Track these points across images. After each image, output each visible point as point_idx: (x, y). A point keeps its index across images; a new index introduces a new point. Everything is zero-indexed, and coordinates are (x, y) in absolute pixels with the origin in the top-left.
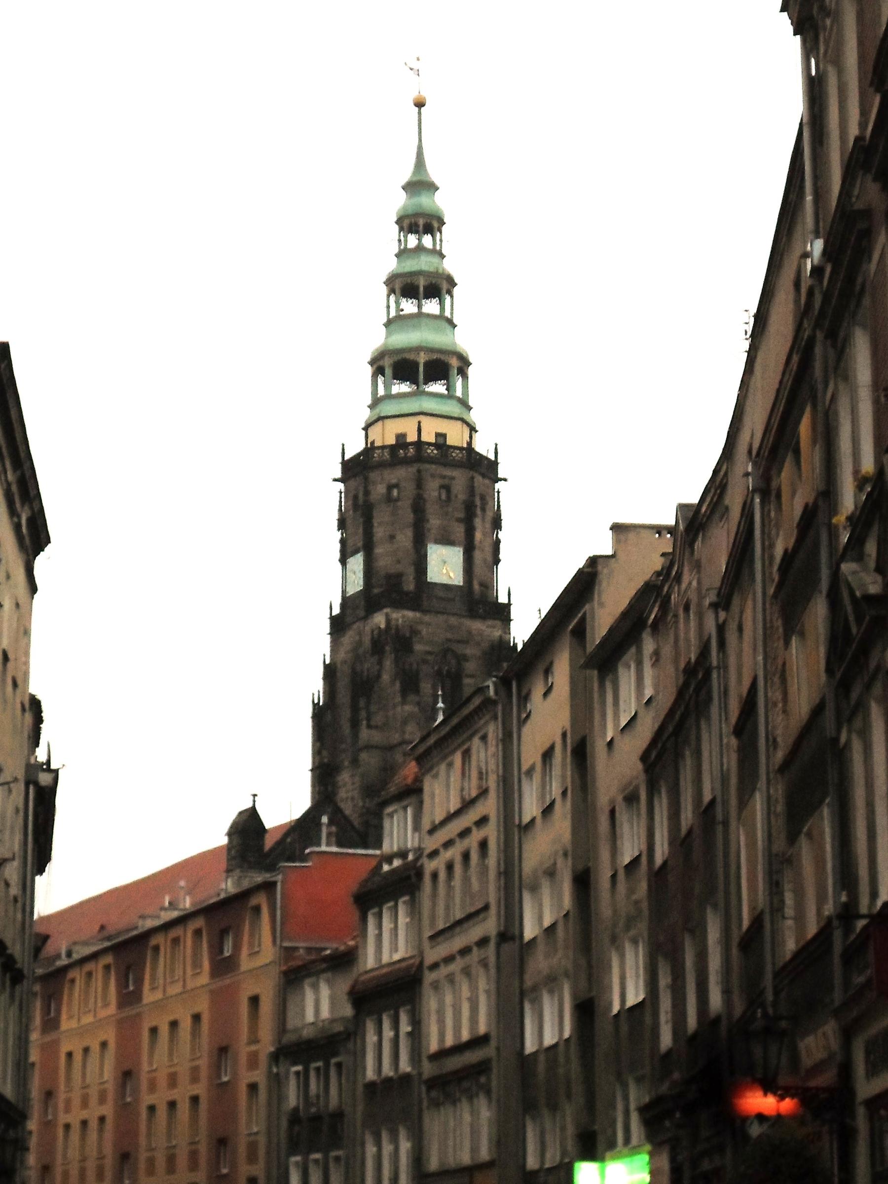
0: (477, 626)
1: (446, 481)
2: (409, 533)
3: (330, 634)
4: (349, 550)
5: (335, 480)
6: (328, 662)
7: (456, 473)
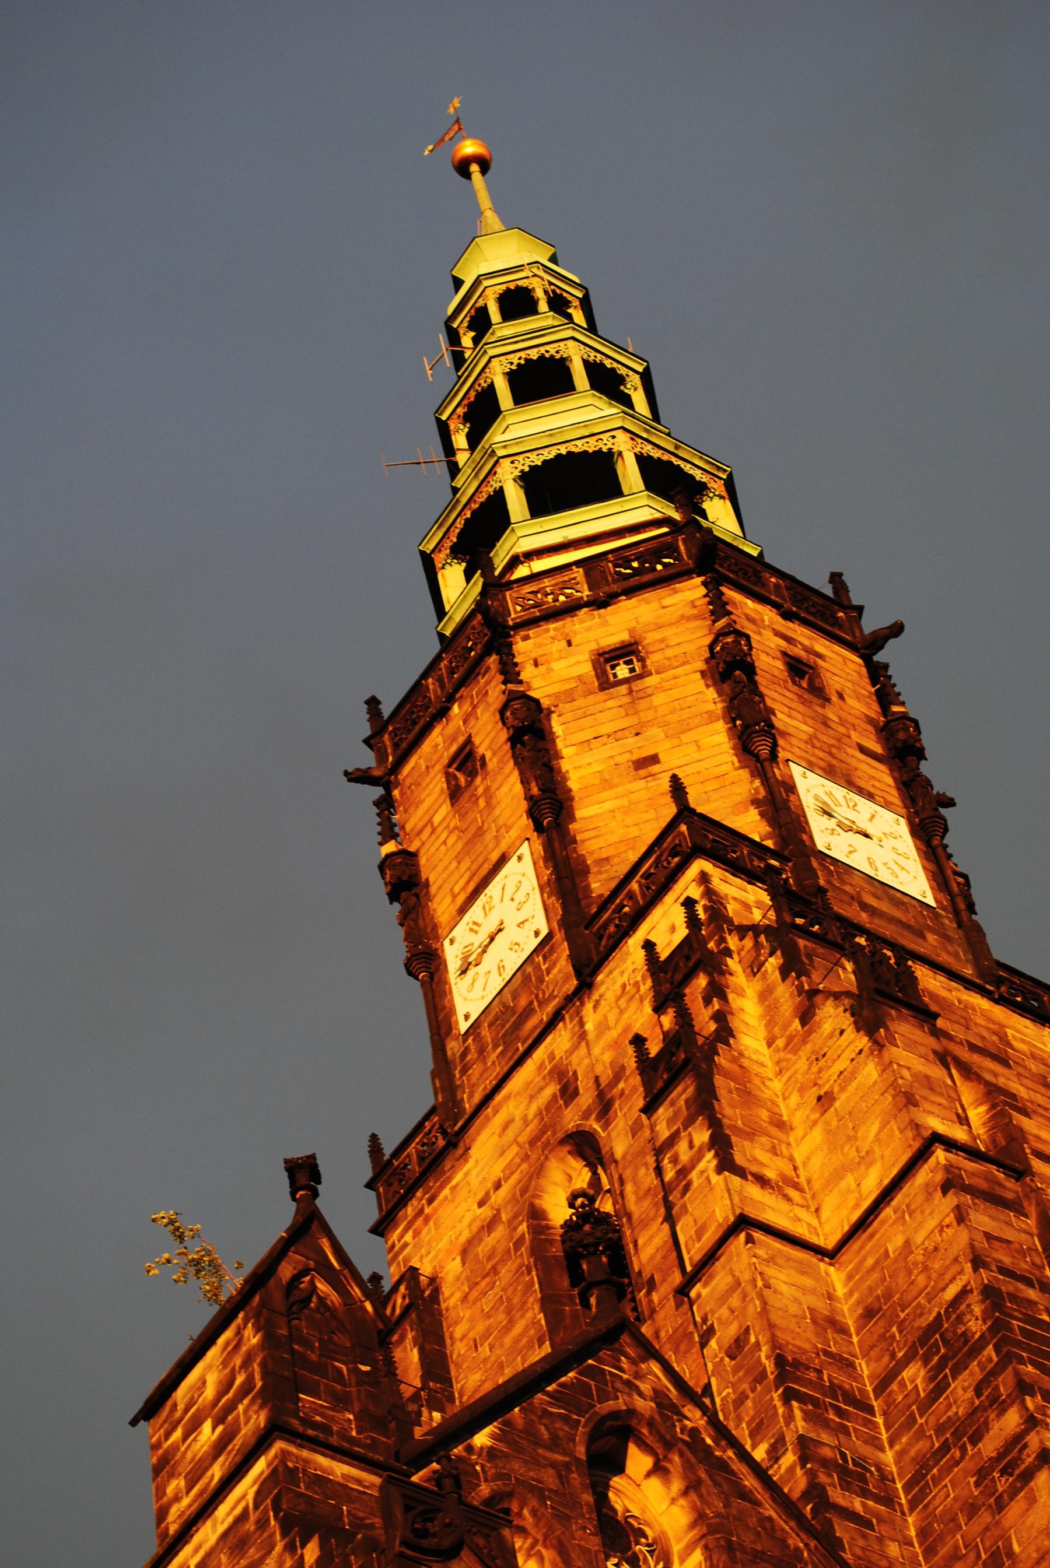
1: (798, 651)
7: (821, 645)
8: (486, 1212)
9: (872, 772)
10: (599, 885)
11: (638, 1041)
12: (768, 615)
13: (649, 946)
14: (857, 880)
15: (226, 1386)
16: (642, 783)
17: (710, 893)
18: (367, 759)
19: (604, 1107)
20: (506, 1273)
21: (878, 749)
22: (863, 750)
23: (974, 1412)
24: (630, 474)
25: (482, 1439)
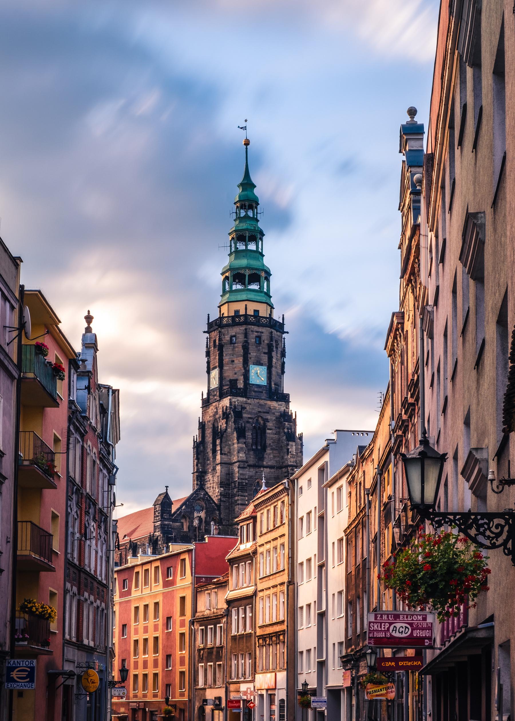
0: (274, 404)
2: (241, 359)
4: (211, 367)
5: (204, 332)
6: (201, 421)
9: (264, 358)
16: (231, 365)
25: (184, 507)
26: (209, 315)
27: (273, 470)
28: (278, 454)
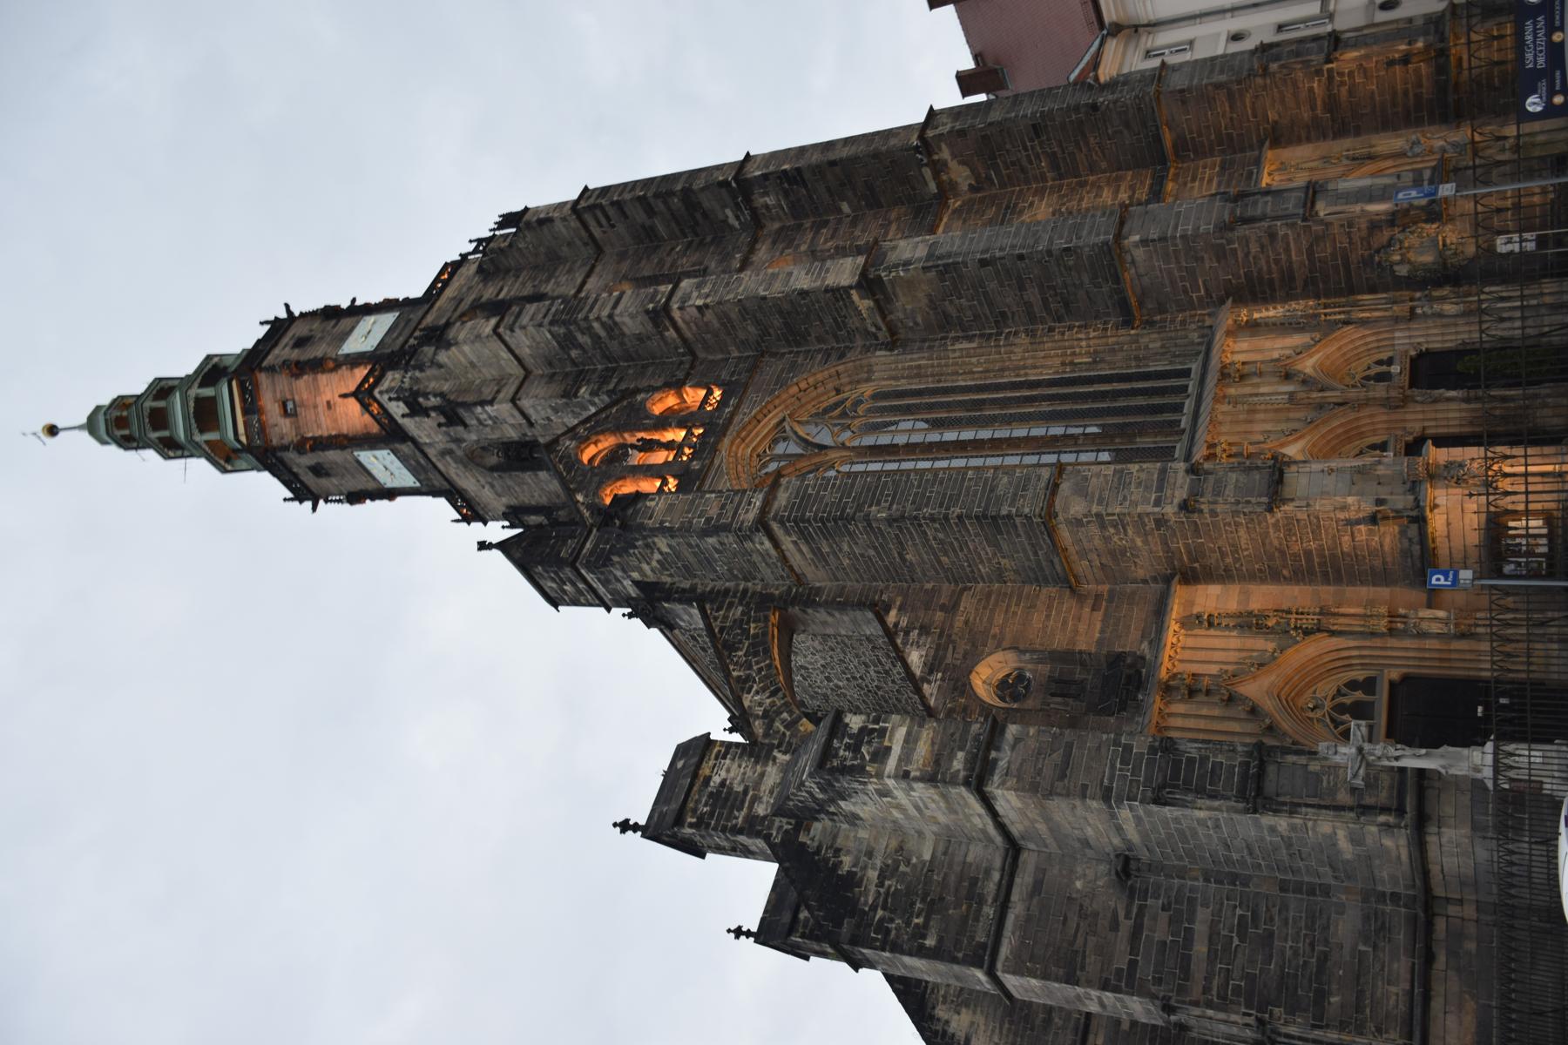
1: (291, 343)
3: (485, 524)
4: (371, 486)
5: (314, 509)
7: (290, 334)
8: (487, 487)
10: (375, 428)
11: (440, 425)
12: (276, 351)
13: (403, 416)
14: (388, 340)
15: (553, 580)
17: (387, 391)
18: (308, 504)
19: (458, 441)
20: (510, 483)
21: (333, 322)
22: (334, 327)
23: (591, 337)
24: (208, 392)
26: (285, 500)
27: (598, 269)
28: (568, 265)
